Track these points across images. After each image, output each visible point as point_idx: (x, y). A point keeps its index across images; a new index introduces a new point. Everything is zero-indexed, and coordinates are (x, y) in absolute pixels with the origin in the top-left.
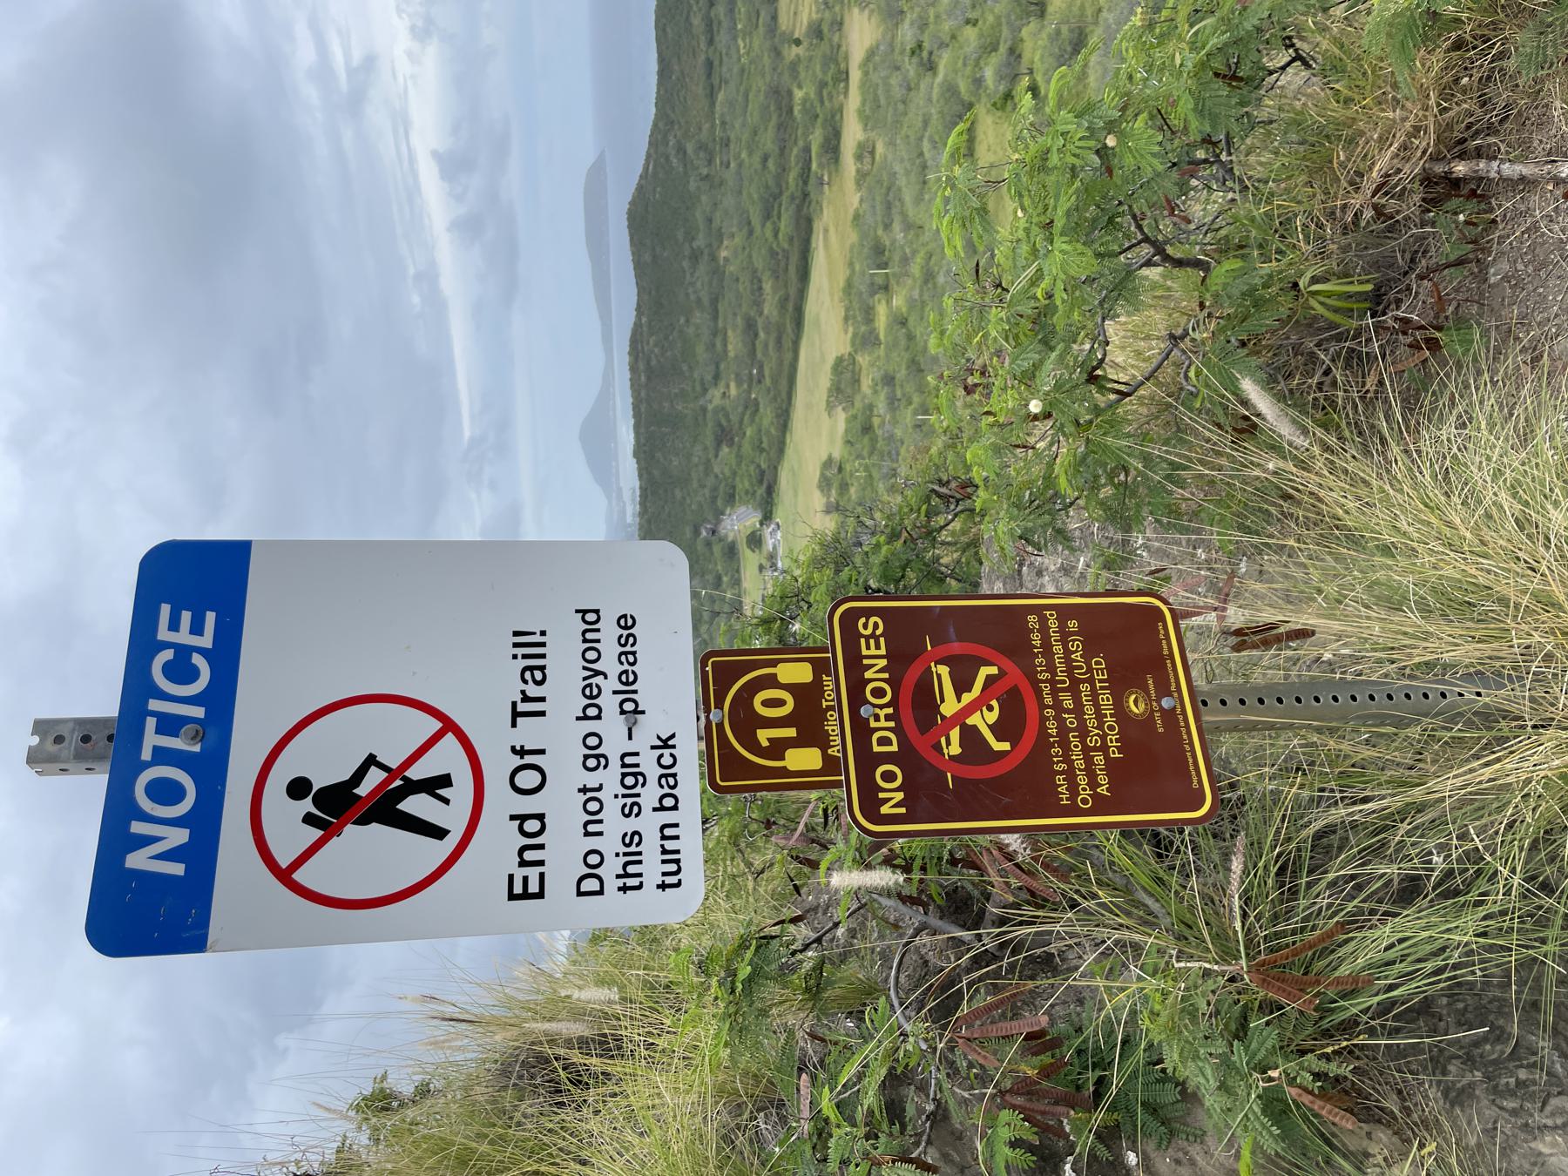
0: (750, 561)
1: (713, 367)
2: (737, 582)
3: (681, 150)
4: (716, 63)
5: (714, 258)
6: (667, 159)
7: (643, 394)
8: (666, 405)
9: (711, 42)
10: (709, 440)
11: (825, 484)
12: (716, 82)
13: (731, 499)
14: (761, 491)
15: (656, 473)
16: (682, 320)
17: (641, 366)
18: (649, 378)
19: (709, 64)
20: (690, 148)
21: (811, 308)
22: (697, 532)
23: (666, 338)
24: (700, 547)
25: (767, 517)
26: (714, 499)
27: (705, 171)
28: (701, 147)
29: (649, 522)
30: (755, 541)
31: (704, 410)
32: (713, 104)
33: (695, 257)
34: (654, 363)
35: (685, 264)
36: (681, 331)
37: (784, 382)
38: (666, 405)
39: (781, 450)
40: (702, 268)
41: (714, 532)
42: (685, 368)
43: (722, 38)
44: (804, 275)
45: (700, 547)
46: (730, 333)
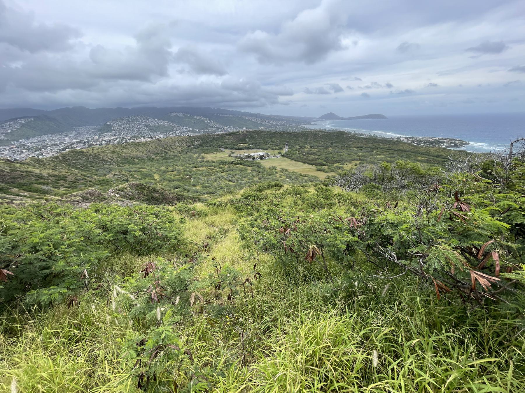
0: (277, 152)
3: (351, 141)
11: (273, 167)
14: (286, 155)
20: (350, 143)
21: (306, 165)
25: (282, 156)
28: (350, 145)
30: (280, 153)
32: (356, 148)
39: (290, 159)
44: (310, 164)
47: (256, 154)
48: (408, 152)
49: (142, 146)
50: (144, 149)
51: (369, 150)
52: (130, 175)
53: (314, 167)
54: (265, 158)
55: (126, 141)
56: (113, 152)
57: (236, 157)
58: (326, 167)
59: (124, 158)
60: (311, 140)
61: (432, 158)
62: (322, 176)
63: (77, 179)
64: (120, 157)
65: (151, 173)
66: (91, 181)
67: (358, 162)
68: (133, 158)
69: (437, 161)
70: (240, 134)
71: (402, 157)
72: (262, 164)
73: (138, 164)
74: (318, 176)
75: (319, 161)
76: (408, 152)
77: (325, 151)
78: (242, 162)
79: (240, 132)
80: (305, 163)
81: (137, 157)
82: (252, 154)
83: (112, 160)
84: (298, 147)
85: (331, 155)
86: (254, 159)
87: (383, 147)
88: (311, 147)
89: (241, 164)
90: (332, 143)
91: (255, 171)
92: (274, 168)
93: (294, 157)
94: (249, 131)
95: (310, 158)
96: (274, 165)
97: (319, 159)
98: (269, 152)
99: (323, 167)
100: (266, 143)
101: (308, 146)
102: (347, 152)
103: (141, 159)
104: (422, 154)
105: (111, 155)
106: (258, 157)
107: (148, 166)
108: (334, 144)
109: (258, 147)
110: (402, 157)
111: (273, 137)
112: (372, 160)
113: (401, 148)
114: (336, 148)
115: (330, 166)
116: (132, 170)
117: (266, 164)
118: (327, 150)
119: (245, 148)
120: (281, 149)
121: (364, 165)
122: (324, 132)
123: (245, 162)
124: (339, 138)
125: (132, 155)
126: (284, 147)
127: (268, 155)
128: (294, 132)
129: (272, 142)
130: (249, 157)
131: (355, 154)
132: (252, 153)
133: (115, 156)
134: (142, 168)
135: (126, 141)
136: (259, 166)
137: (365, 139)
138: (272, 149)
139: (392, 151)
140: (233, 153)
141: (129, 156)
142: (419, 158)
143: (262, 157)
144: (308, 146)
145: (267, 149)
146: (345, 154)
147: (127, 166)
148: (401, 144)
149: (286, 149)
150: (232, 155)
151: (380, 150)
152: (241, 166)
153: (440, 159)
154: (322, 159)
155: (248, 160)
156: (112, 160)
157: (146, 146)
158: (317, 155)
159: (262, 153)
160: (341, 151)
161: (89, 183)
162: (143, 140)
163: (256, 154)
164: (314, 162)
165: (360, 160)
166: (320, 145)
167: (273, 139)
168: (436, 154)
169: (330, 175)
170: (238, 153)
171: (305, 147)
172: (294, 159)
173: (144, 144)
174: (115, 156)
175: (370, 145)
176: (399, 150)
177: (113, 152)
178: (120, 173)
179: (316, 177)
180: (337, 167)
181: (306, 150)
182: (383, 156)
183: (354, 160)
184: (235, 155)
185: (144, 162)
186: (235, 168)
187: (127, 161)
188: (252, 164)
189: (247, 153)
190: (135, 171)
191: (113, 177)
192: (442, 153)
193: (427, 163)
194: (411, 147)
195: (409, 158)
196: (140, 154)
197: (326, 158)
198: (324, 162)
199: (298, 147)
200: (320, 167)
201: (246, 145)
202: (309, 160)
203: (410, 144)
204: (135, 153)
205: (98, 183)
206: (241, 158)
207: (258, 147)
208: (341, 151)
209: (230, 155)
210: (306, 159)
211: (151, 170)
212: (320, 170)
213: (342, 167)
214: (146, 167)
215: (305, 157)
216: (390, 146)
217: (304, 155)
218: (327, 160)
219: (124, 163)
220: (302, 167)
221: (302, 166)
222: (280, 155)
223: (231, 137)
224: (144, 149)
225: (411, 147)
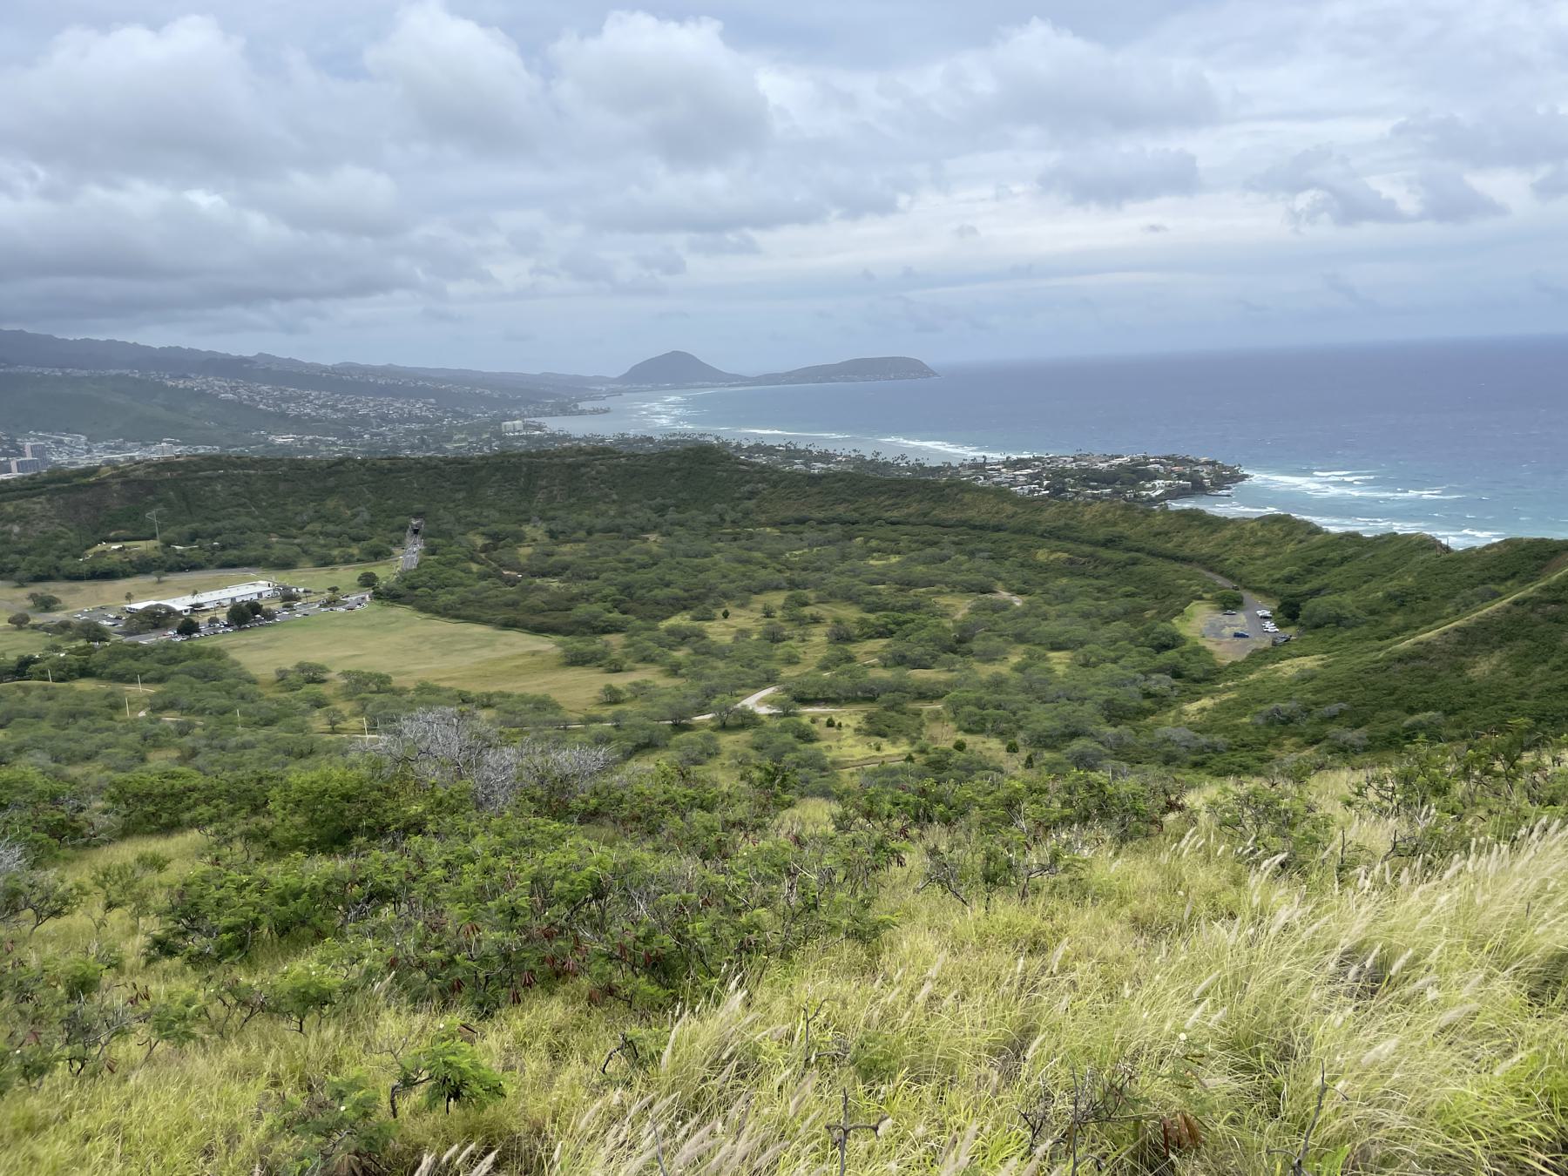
0: (347, 576)
1: (560, 528)
2: (348, 561)
3: (751, 495)
4: (800, 528)
5: (655, 528)
6: (748, 482)
7: (556, 460)
8: (544, 483)
9: (821, 522)
10: (495, 528)
11: (302, 667)
12: (787, 528)
13: (432, 551)
15: (483, 473)
16: (615, 497)
17: (582, 459)
18: (569, 466)
19: (802, 521)
20: (751, 504)
22: (417, 515)
23: (603, 482)
24: (400, 520)
25: (378, 596)
26: (441, 534)
27: (727, 518)
28: (746, 514)
29: (436, 467)
30: (368, 581)
31: (528, 521)
32: (774, 525)
33: (661, 510)
34: (583, 470)
35: (659, 500)
36: (606, 495)
37: (470, 611)
38: (544, 483)
39: (423, 609)
40: (654, 517)
41: (416, 532)
42: (572, 500)
43: (810, 534)
44: (538, 630)
45: (400, 520)
46: (582, 545)
47: (207, 598)
48: (997, 529)
51: (836, 530)
53: (547, 645)
54: (269, 616)
57: (65, 626)
58: (616, 640)
60: (551, 499)
61: (1087, 549)
62: (579, 690)
67: (777, 599)
69: (1107, 563)
70: (102, 483)
71: (972, 554)
72: (234, 655)
74: (556, 696)
75: (582, 610)
76: (997, 529)
77: (626, 554)
78: (98, 657)
79: (106, 472)
80: (508, 625)
82: (181, 604)
84: (480, 541)
85: (651, 574)
86: (188, 628)
87: (895, 514)
88: (552, 534)
89: (85, 673)
90: (661, 510)
91: (170, 706)
92: (313, 674)
93: (444, 598)
94: (167, 465)
95: (535, 599)
96: (315, 657)
97: (585, 597)
98: (302, 579)
99: (600, 642)
100: (282, 528)
101: (535, 531)
102: (735, 549)
104: (1052, 534)
106: (222, 616)
108: (672, 515)
109: (232, 554)
110: (972, 554)
111: (331, 492)
112: (845, 580)
113: (971, 513)
114: (679, 531)
115: (637, 632)
117: (259, 656)
118: (638, 544)
119: (143, 567)
120: (378, 555)
121: (807, 611)
122: (619, 455)
123: (118, 653)
124: (693, 478)
126: (400, 543)
127: (288, 598)
128: (455, 461)
129: (327, 519)
130: (157, 619)
131: (773, 556)
132: (184, 590)
136: (211, 669)
137: (814, 480)
138: (325, 562)
139: (930, 532)
140: (47, 604)
142: (1042, 556)
143: (244, 615)
144: (535, 531)
145: (286, 565)
146: (722, 559)
148: (968, 497)
149: (409, 556)
150: (37, 619)
151: (880, 532)
152: (84, 685)
153: (1119, 556)
154: (604, 599)
155: (146, 640)
158: (579, 577)
159: (252, 587)
160: (705, 545)
163: (207, 598)
164: (548, 620)
165: (793, 585)
166: (599, 523)
167: (330, 503)
168: (1102, 533)
169: (620, 681)
170: (81, 603)
171: (519, 538)
172: (446, 612)
175: (840, 509)
176: (963, 523)
179: (542, 705)
180: (671, 632)
181: (525, 551)
182: (894, 559)
183: (759, 592)
184: (59, 616)
186: (33, 702)
188: (164, 665)
189: (145, 594)
192: (1123, 528)
193: (1072, 574)
194: (1009, 509)
195: (998, 557)
197: (627, 588)
198: (616, 615)
199: (480, 541)
200: (577, 644)
201: (143, 546)
202: (534, 610)
203: (1001, 493)
206: (94, 632)
207: (232, 554)
208: (705, 545)
209: (19, 622)
210: (514, 604)
212: (576, 660)
213: (701, 635)
215: (511, 593)
216: (926, 506)
217: (512, 582)
218: (627, 598)
220: (487, 653)
221: (490, 644)
222: (367, 595)
223: (38, 505)
225: (1009, 509)
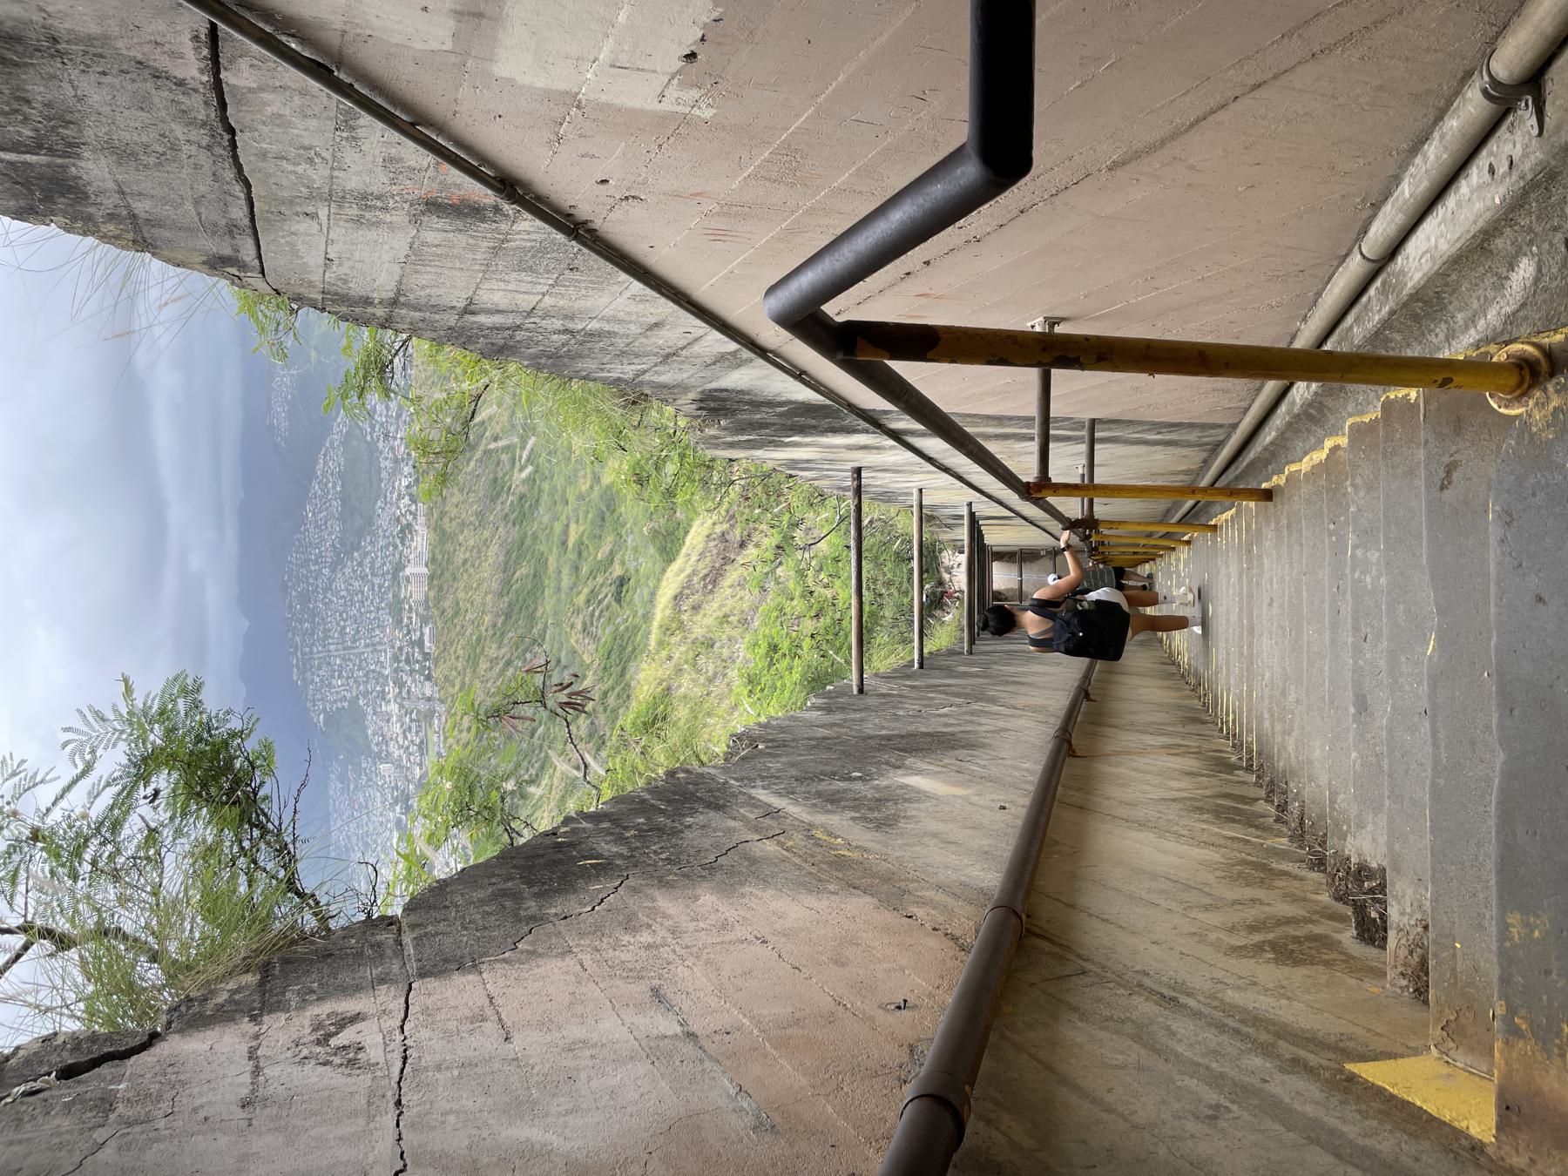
49: (449, 547)
50: (469, 538)
52: (592, 575)
55: (412, 644)
56: (473, 661)
59: (508, 616)
63: (591, 736)
64: (499, 635)
65: (596, 494)
66: (605, 694)
68: (506, 584)
73: (542, 561)
81: (507, 568)
83: (508, 663)
103: (517, 552)
105: (484, 665)
107: (556, 518)
116: (566, 581)
125: (495, 586)
133: (492, 652)
134: (564, 543)
135: (412, 644)
141: (501, 595)
147: (547, 605)
156: (508, 663)
157: (448, 527)
161: (611, 700)
162: (416, 569)
173: (442, 537)
174: (492, 652)
177: (473, 661)
178: (578, 611)
185: (535, 537)
187: (520, 604)
190: (577, 569)
191: (596, 639)
196: (494, 553)
204: (488, 572)
205: (615, 671)
211: (581, 497)
214: (558, 528)
219: (532, 617)
224: (469, 538)
